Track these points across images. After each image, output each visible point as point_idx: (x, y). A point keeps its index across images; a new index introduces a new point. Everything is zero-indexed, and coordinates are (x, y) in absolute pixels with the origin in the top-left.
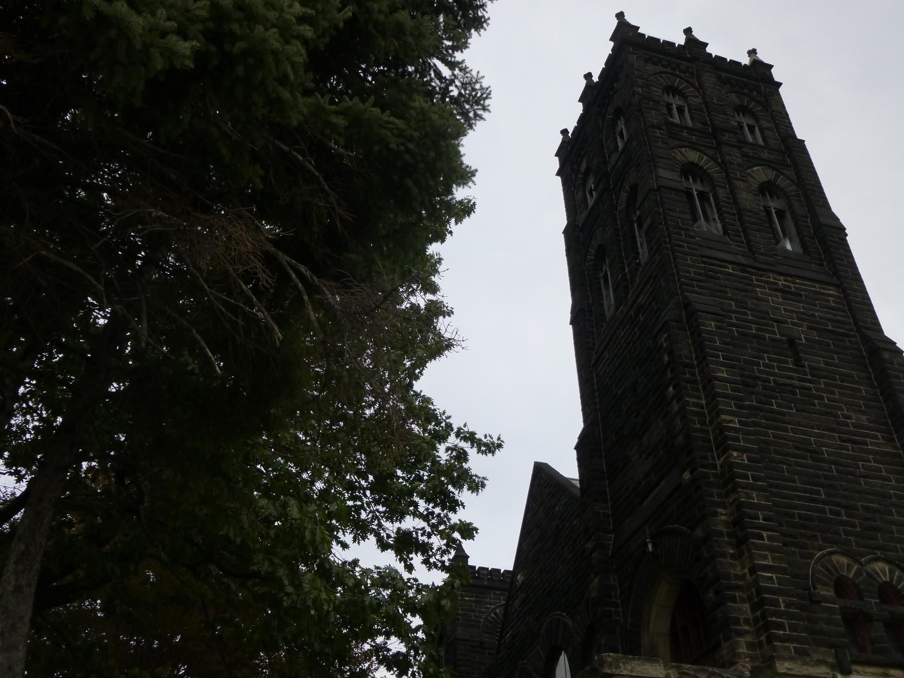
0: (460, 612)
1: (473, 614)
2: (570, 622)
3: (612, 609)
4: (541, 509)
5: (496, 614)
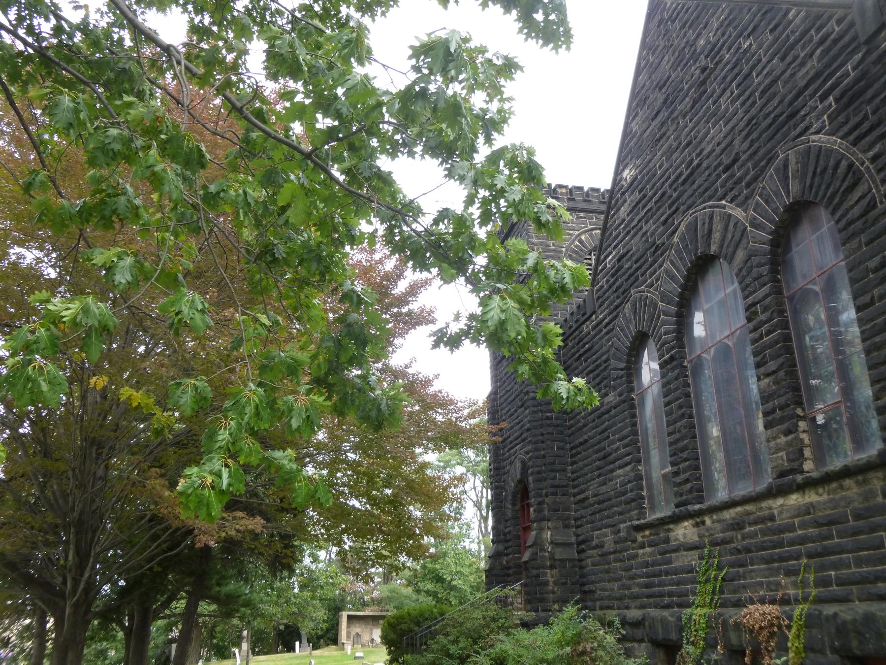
2: (738, 213)
4: (666, 58)
5: (581, 241)
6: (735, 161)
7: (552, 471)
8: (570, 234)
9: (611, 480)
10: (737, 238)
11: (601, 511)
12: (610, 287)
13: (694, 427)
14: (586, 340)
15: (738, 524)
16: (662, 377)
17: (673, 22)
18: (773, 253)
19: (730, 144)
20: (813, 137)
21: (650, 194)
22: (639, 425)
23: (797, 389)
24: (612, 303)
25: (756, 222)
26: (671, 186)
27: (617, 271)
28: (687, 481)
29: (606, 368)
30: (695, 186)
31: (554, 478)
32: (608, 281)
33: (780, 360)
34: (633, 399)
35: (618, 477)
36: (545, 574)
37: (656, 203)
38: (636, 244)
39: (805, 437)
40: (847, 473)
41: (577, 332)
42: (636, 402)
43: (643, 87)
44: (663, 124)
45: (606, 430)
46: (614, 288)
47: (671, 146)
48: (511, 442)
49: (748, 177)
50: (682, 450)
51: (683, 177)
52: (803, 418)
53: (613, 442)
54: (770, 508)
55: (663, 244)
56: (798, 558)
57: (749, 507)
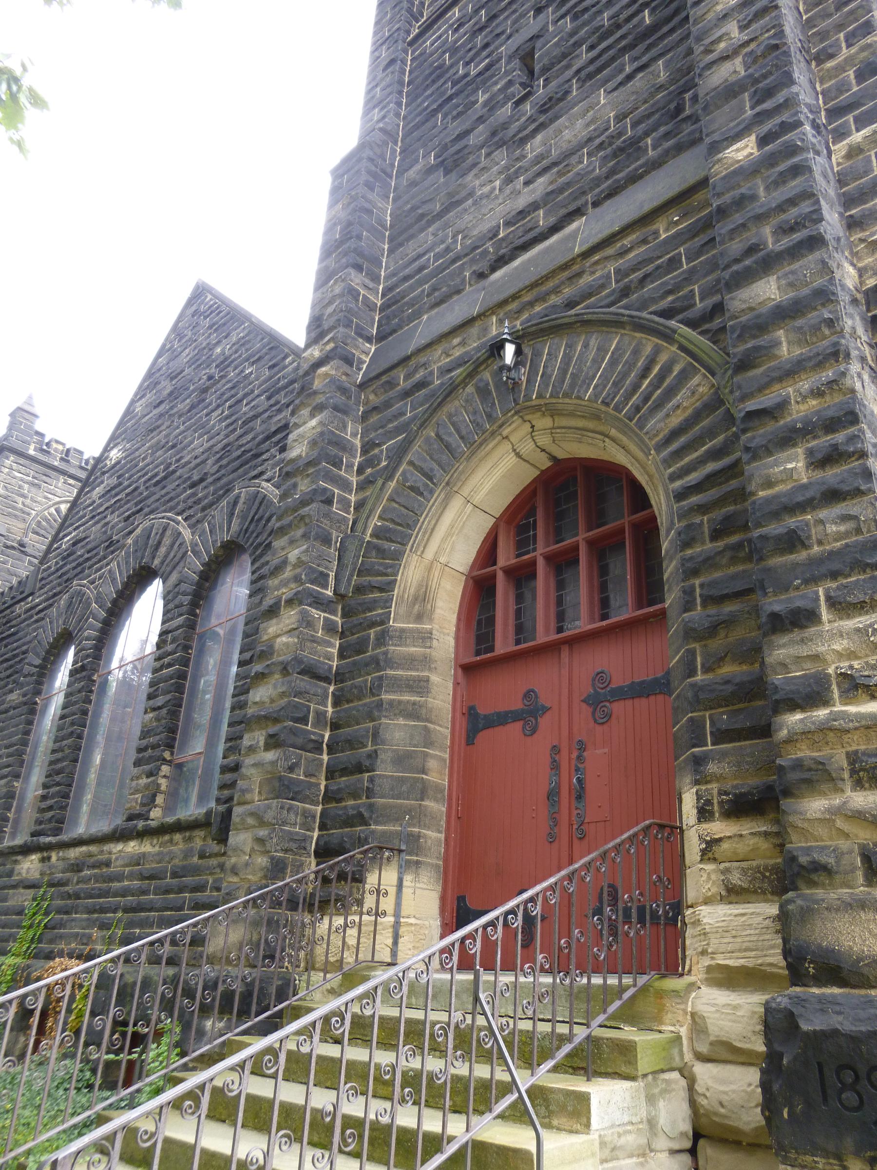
1: (20, 500)
2: (187, 534)
3: (336, 491)
4: (187, 351)
5: (58, 511)
6: (202, 480)
10: (177, 559)
12: (57, 570)
13: (80, 749)
14: (14, 623)
15: (77, 865)
16: (68, 686)
17: (205, 318)
18: (199, 585)
19: (204, 462)
20: (264, 484)
21: (126, 483)
22: (32, 735)
23: (172, 730)
24: (51, 590)
25: (197, 549)
26: (145, 482)
27: (69, 555)
28: (50, 808)
29: (22, 660)
30: (163, 492)
32: (57, 563)
34: (36, 703)
37: (127, 495)
38: (95, 531)
40: (178, 827)
42: (39, 708)
43: (159, 370)
44: (161, 415)
46: (59, 573)
47: (159, 441)
49: (206, 501)
51: (157, 478)
52: (169, 763)
54: (110, 853)
55: (118, 541)
56: (115, 911)
57: (93, 848)
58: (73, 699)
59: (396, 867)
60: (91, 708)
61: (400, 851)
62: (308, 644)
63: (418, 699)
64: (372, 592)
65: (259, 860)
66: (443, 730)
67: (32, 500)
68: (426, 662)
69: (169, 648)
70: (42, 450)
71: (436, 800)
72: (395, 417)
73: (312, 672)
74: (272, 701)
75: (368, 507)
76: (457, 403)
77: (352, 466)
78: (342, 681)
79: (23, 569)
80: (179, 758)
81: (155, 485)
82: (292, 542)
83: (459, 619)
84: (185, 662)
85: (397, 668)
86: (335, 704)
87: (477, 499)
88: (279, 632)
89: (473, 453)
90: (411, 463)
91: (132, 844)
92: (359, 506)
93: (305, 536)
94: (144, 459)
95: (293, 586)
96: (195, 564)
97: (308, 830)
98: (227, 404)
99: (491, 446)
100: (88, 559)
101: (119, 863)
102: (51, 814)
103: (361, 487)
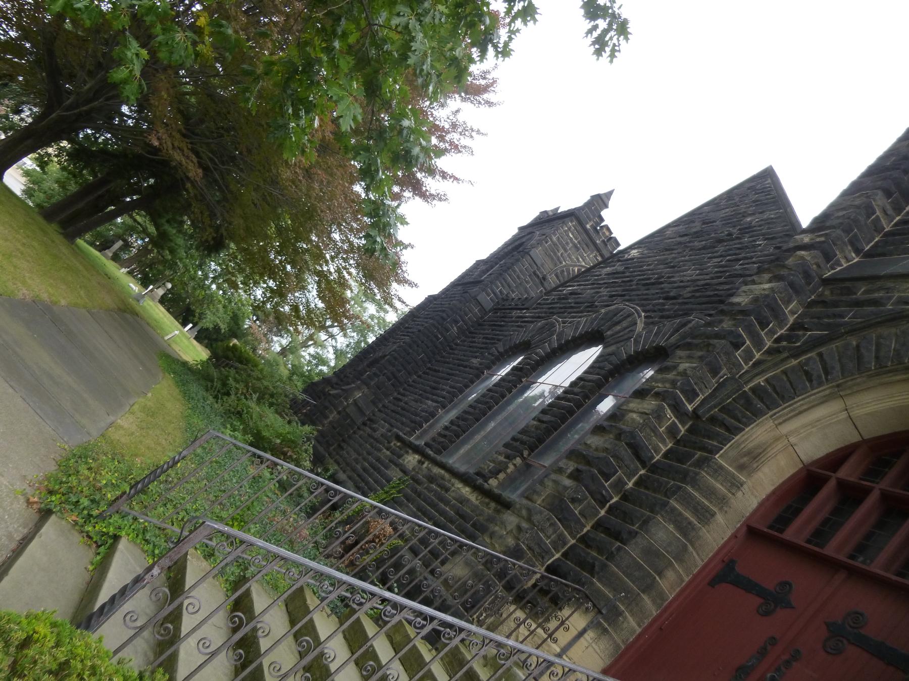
0: (554, 239)
1: (562, 251)
2: (640, 326)
3: (748, 342)
4: (728, 210)
6: (674, 298)
7: (402, 365)
8: (578, 259)
9: (421, 403)
11: (398, 413)
14: (506, 319)
15: (433, 478)
17: (755, 194)
21: (627, 274)
22: (468, 390)
23: (541, 441)
27: (564, 299)
28: (445, 436)
29: (495, 343)
31: (399, 371)
32: (554, 299)
33: (553, 419)
34: (483, 373)
35: (426, 404)
36: (331, 412)
37: (623, 282)
39: (511, 468)
41: (508, 311)
44: (680, 243)
45: (453, 375)
47: (667, 259)
48: (408, 332)
49: (667, 313)
50: (464, 420)
52: (523, 459)
53: (446, 385)
54: (453, 485)
55: (596, 307)
57: (447, 476)
58: (503, 384)
59: (589, 620)
60: (508, 396)
61: (600, 612)
62: (648, 430)
63: (696, 522)
64: (720, 427)
65: (510, 540)
66: (699, 558)
67: (569, 256)
68: (723, 502)
69: (576, 390)
70: (595, 229)
71: (654, 602)
72: (835, 316)
73: (637, 450)
74: (597, 449)
75: (763, 367)
76: (893, 330)
77: (775, 333)
78: (653, 472)
79: (535, 292)
80: (532, 461)
81: (644, 285)
82: (690, 357)
83: (774, 492)
84: (579, 405)
85: (697, 490)
86: (636, 484)
87: (856, 413)
88: (635, 409)
89: (878, 375)
90: (820, 355)
91: (467, 489)
92: (758, 363)
93: (701, 358)
94: (649, 265)
95: (667, 385)
96: (631, 348)
97: (554, 549)
98: (728, 258)
99: (898, 378)
100: (572, 307)
101: (453, 494)
102: (443, 440)
103: (770, 352)
